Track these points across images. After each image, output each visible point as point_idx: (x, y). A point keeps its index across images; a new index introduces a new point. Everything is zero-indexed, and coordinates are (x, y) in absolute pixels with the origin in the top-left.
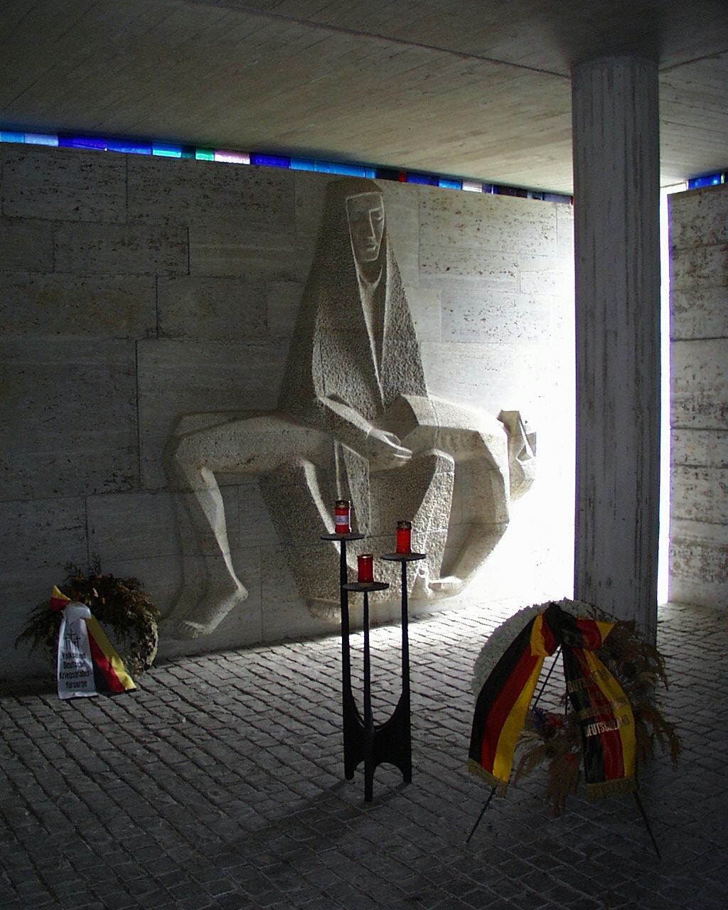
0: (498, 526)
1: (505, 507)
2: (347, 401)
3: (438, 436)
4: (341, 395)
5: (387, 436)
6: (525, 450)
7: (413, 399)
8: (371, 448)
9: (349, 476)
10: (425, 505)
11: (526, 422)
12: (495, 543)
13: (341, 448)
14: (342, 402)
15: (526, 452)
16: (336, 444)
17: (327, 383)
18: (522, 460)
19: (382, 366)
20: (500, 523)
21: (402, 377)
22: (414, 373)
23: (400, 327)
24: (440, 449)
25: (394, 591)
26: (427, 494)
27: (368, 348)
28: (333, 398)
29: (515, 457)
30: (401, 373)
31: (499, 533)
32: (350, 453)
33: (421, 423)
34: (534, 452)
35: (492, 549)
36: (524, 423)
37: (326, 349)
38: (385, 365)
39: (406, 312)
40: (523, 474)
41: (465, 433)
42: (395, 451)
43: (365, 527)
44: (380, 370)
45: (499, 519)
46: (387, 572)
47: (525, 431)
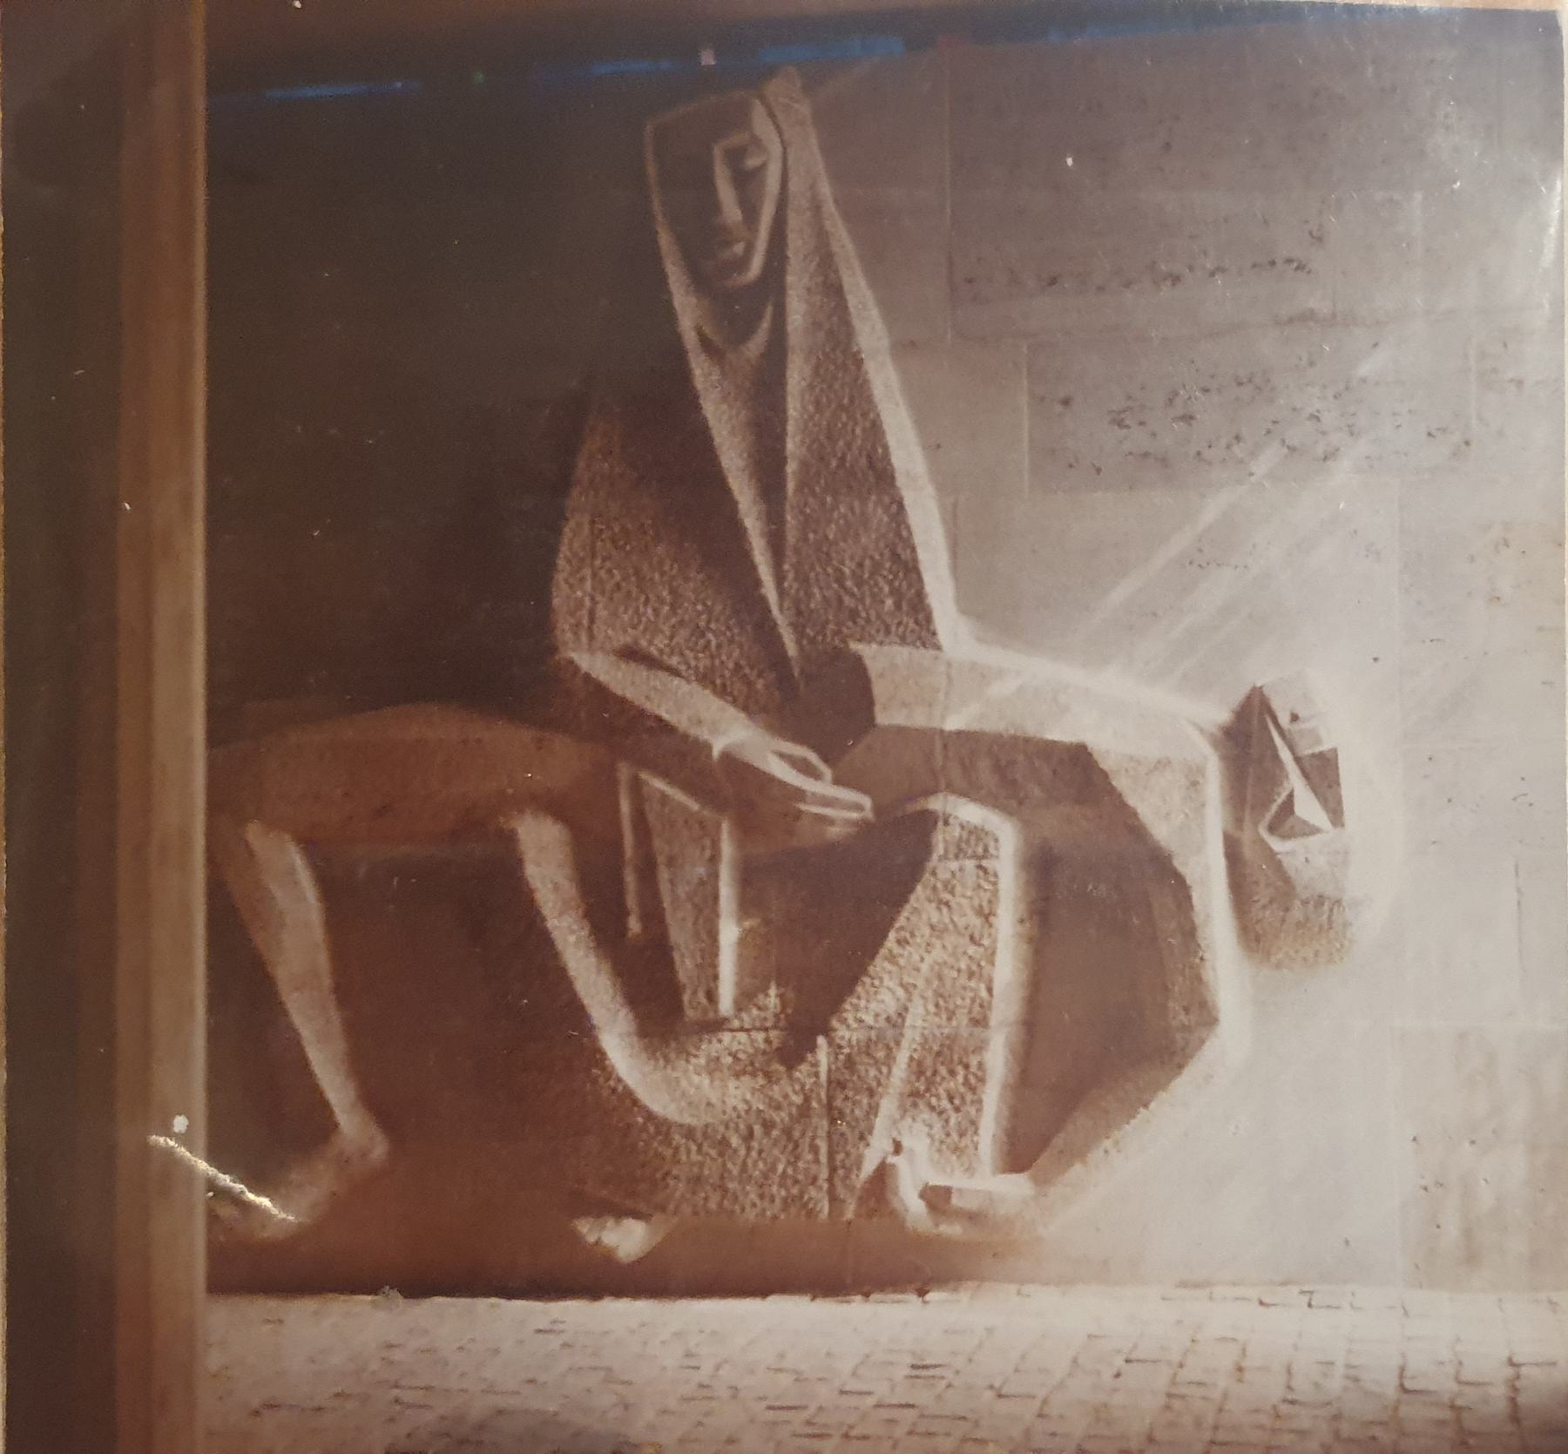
0: (1178, 1036)
1: (1199, 979)
2: (674, 661)
3: (946, 757)
4: (656, 645)
5: (782, 756)
6: (1288, 806)
7: (878, 657)
8: (736, 790)
9: (661, 859)
10: (896, 950)
11: (1295, 718)
12: (1160, 1085)
13: (636, 786)
14: (651, 662)
15: (1292, 812)
16: (624, 772)
17: (602, 613)
18: (1285, 837)
19: (786, 567)
20: (1185, 1028)
21: (852, 595)
22: (891, 583)
23: (843, 459)
24: (963, 794)
25: (795, 1191)
26: (901, 921)
27: (738, 531)
28: (631, 654)
29: (1256, 824)
30: (849, 583)
31: (1177, 1060)
32: (664, 798)
33: (882, 718)
34: (1336, 814)
35: (1146, 1106)
36: (1284, 720)
37: (609, 528)
38: (797, 567)
39: (864, 415)
40: (1287, 880)
41: (1048, 750)
42: (800, 794)
43: (704, 1001)
44: (779, 578)
45: (1182, 1017)
46: (767, 1133)
47: (1292, 749)
